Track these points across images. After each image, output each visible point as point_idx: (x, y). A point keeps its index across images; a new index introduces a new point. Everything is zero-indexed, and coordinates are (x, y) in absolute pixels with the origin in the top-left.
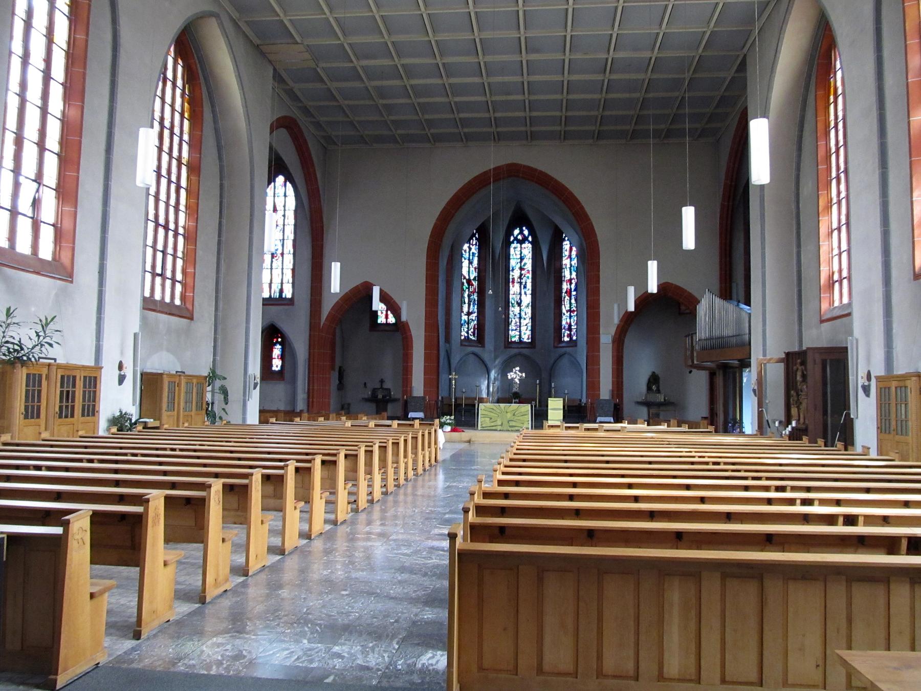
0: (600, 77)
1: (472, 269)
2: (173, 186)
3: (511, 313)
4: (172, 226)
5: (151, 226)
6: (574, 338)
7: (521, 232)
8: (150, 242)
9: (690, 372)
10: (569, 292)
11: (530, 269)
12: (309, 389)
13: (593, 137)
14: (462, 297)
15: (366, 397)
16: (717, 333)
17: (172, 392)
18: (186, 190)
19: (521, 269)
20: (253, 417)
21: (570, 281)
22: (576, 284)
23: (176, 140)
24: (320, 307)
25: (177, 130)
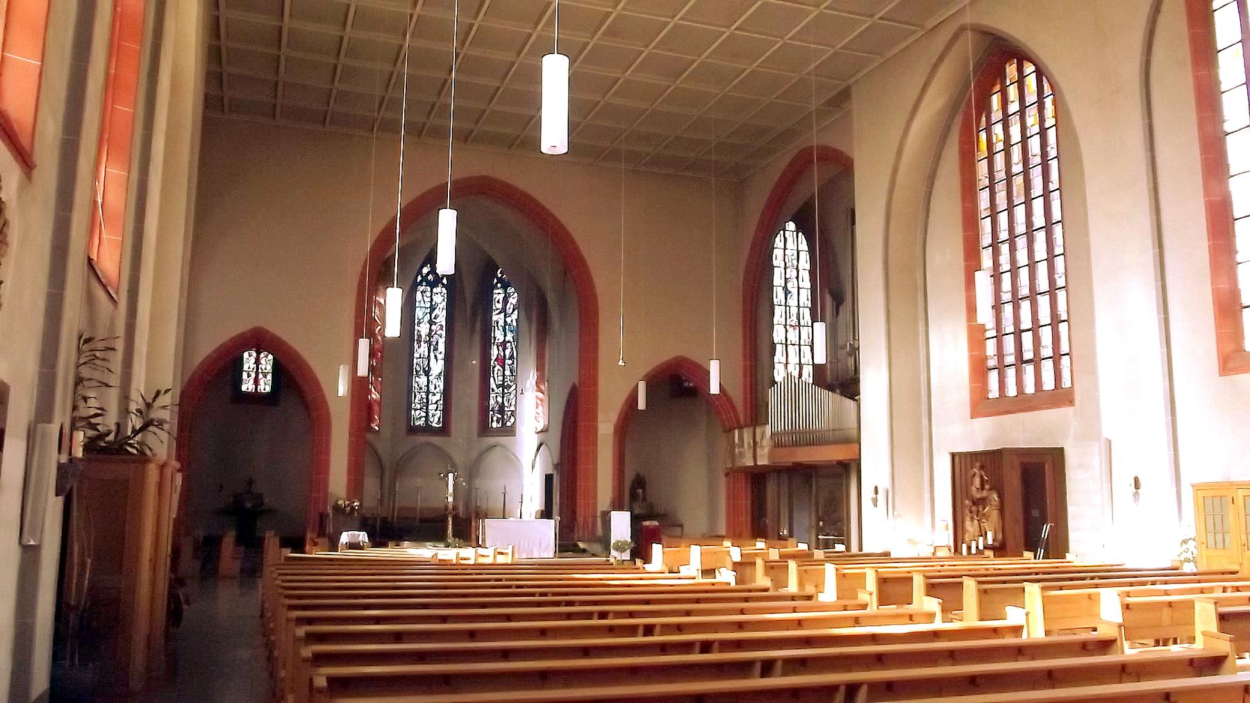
10: (501, 360)
16: (802, 425)
19: (431, 323)
21: (504, 344)
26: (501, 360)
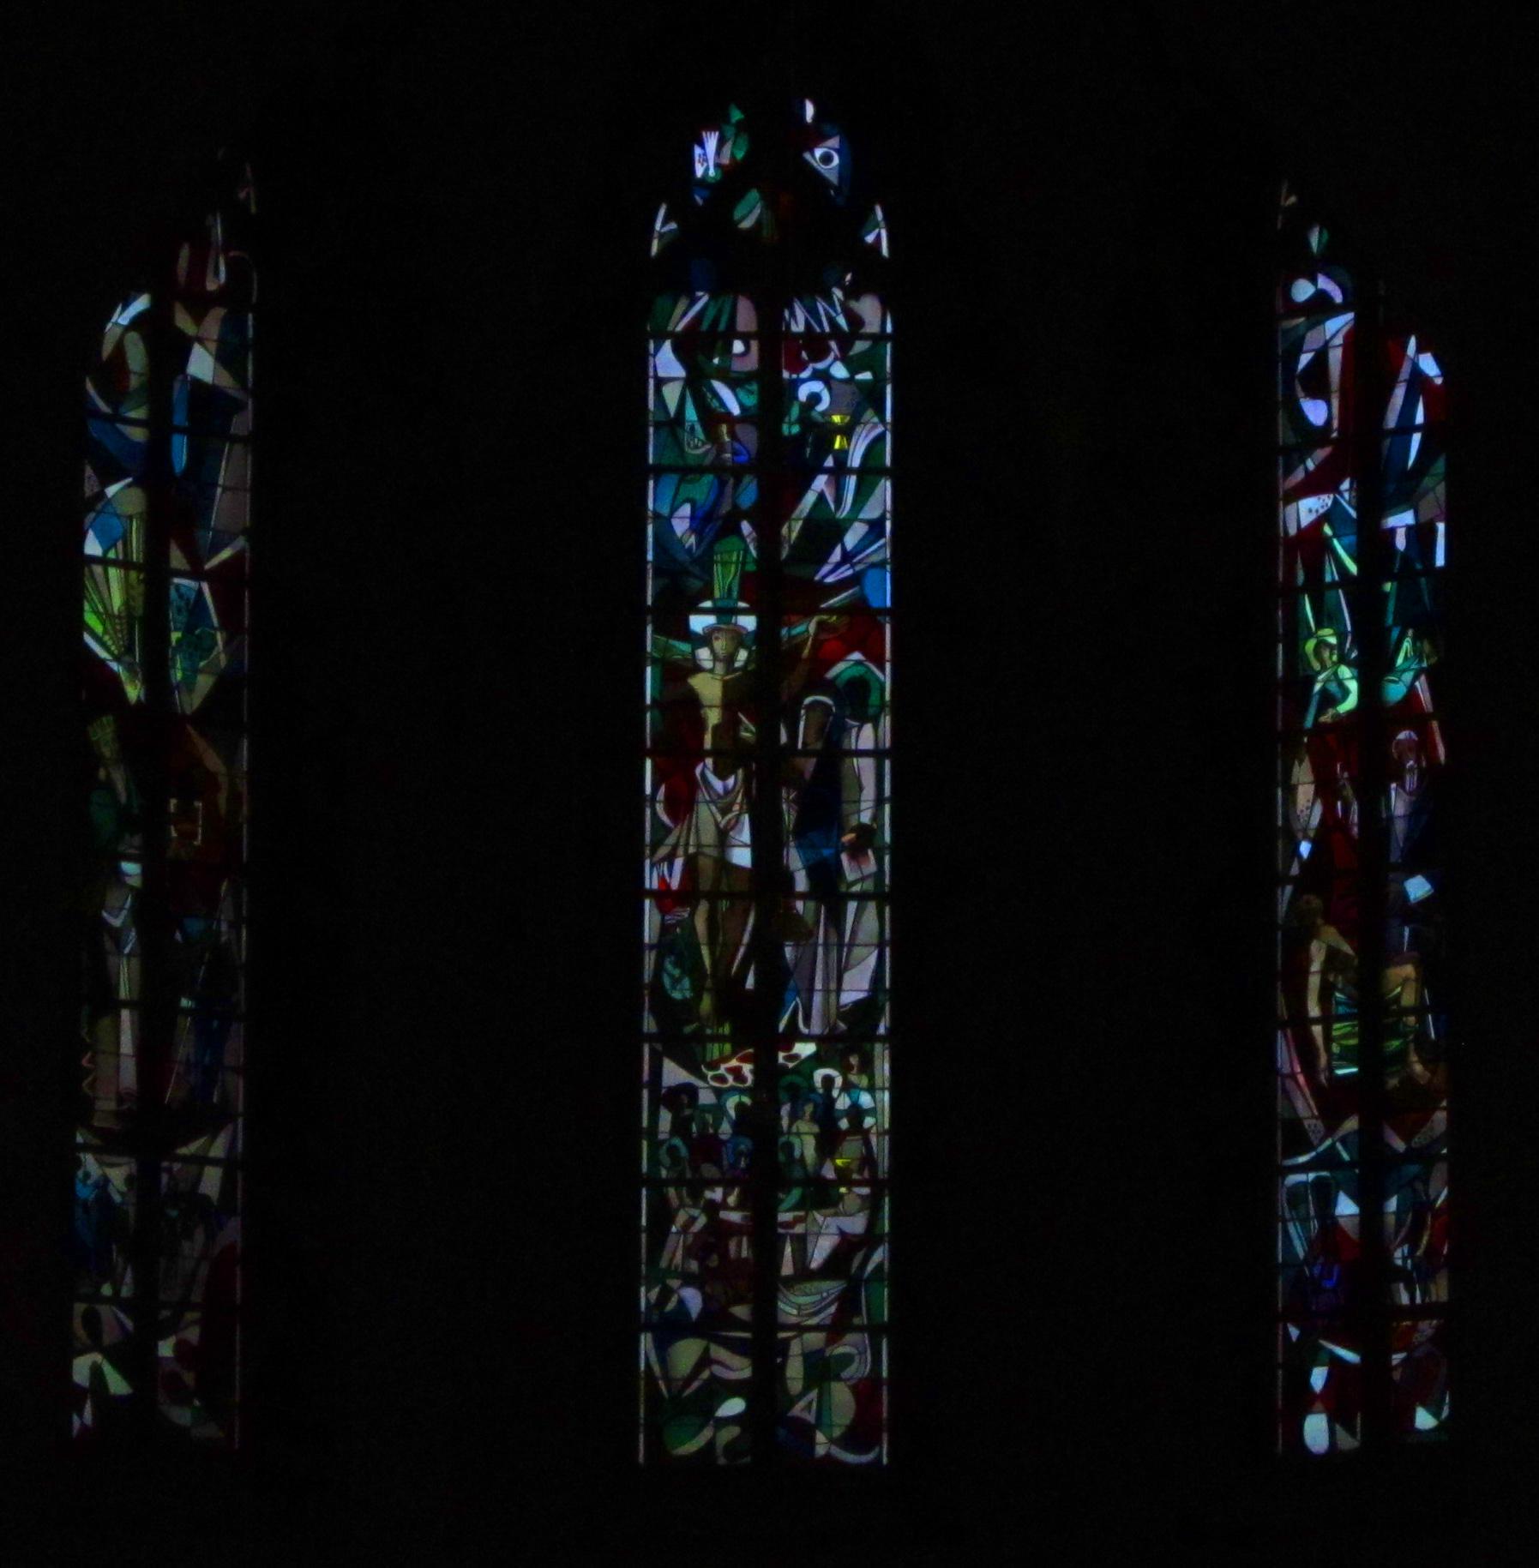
7: (772, 159)
10: (1353, 873)
19: (778, 588)
21: (1362, 748)
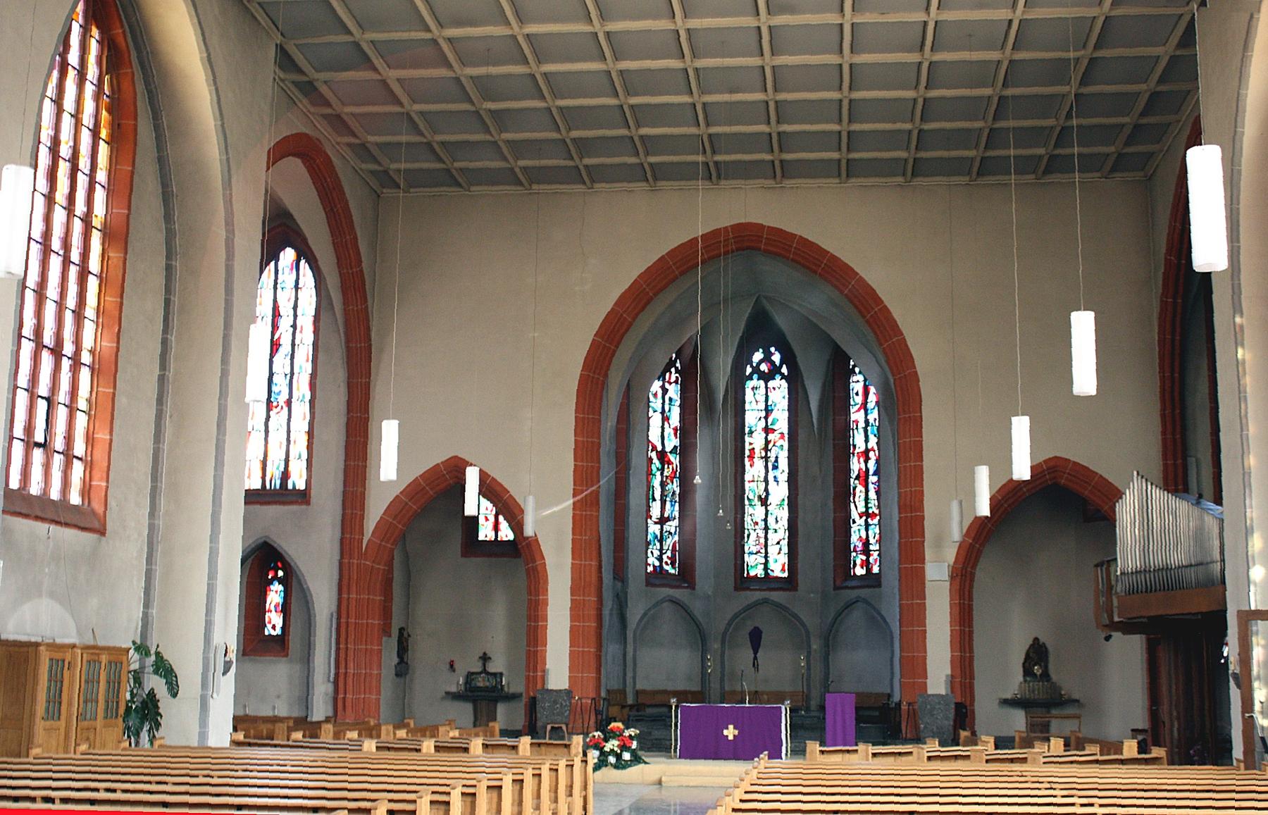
0: (913, 58)
1: (669, 431)
2: (73, 271)
3: (747, 519)
4: (68, 349)
5: (27, 347)
6: (876, 570)
7: (767, 358)
8: (23, 380)
9: (1108, 638)
10: (864, 477)
11: (786, 432)
12: (337, 675)
13: (904, 175)
14: (649, 486)
15: (454, 689)
16: (1156, 560)
17: (56, 680)
18: (100, 277)
19: (767, 430)
20: (220, 733)
21: (866, 454)
22: (877, 461)
23: (82, 180)
24: (363, 508)
25: (84, 163)
26: (864, 477)
